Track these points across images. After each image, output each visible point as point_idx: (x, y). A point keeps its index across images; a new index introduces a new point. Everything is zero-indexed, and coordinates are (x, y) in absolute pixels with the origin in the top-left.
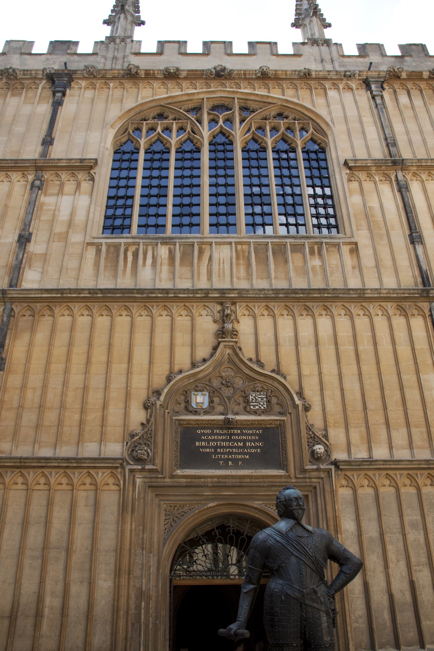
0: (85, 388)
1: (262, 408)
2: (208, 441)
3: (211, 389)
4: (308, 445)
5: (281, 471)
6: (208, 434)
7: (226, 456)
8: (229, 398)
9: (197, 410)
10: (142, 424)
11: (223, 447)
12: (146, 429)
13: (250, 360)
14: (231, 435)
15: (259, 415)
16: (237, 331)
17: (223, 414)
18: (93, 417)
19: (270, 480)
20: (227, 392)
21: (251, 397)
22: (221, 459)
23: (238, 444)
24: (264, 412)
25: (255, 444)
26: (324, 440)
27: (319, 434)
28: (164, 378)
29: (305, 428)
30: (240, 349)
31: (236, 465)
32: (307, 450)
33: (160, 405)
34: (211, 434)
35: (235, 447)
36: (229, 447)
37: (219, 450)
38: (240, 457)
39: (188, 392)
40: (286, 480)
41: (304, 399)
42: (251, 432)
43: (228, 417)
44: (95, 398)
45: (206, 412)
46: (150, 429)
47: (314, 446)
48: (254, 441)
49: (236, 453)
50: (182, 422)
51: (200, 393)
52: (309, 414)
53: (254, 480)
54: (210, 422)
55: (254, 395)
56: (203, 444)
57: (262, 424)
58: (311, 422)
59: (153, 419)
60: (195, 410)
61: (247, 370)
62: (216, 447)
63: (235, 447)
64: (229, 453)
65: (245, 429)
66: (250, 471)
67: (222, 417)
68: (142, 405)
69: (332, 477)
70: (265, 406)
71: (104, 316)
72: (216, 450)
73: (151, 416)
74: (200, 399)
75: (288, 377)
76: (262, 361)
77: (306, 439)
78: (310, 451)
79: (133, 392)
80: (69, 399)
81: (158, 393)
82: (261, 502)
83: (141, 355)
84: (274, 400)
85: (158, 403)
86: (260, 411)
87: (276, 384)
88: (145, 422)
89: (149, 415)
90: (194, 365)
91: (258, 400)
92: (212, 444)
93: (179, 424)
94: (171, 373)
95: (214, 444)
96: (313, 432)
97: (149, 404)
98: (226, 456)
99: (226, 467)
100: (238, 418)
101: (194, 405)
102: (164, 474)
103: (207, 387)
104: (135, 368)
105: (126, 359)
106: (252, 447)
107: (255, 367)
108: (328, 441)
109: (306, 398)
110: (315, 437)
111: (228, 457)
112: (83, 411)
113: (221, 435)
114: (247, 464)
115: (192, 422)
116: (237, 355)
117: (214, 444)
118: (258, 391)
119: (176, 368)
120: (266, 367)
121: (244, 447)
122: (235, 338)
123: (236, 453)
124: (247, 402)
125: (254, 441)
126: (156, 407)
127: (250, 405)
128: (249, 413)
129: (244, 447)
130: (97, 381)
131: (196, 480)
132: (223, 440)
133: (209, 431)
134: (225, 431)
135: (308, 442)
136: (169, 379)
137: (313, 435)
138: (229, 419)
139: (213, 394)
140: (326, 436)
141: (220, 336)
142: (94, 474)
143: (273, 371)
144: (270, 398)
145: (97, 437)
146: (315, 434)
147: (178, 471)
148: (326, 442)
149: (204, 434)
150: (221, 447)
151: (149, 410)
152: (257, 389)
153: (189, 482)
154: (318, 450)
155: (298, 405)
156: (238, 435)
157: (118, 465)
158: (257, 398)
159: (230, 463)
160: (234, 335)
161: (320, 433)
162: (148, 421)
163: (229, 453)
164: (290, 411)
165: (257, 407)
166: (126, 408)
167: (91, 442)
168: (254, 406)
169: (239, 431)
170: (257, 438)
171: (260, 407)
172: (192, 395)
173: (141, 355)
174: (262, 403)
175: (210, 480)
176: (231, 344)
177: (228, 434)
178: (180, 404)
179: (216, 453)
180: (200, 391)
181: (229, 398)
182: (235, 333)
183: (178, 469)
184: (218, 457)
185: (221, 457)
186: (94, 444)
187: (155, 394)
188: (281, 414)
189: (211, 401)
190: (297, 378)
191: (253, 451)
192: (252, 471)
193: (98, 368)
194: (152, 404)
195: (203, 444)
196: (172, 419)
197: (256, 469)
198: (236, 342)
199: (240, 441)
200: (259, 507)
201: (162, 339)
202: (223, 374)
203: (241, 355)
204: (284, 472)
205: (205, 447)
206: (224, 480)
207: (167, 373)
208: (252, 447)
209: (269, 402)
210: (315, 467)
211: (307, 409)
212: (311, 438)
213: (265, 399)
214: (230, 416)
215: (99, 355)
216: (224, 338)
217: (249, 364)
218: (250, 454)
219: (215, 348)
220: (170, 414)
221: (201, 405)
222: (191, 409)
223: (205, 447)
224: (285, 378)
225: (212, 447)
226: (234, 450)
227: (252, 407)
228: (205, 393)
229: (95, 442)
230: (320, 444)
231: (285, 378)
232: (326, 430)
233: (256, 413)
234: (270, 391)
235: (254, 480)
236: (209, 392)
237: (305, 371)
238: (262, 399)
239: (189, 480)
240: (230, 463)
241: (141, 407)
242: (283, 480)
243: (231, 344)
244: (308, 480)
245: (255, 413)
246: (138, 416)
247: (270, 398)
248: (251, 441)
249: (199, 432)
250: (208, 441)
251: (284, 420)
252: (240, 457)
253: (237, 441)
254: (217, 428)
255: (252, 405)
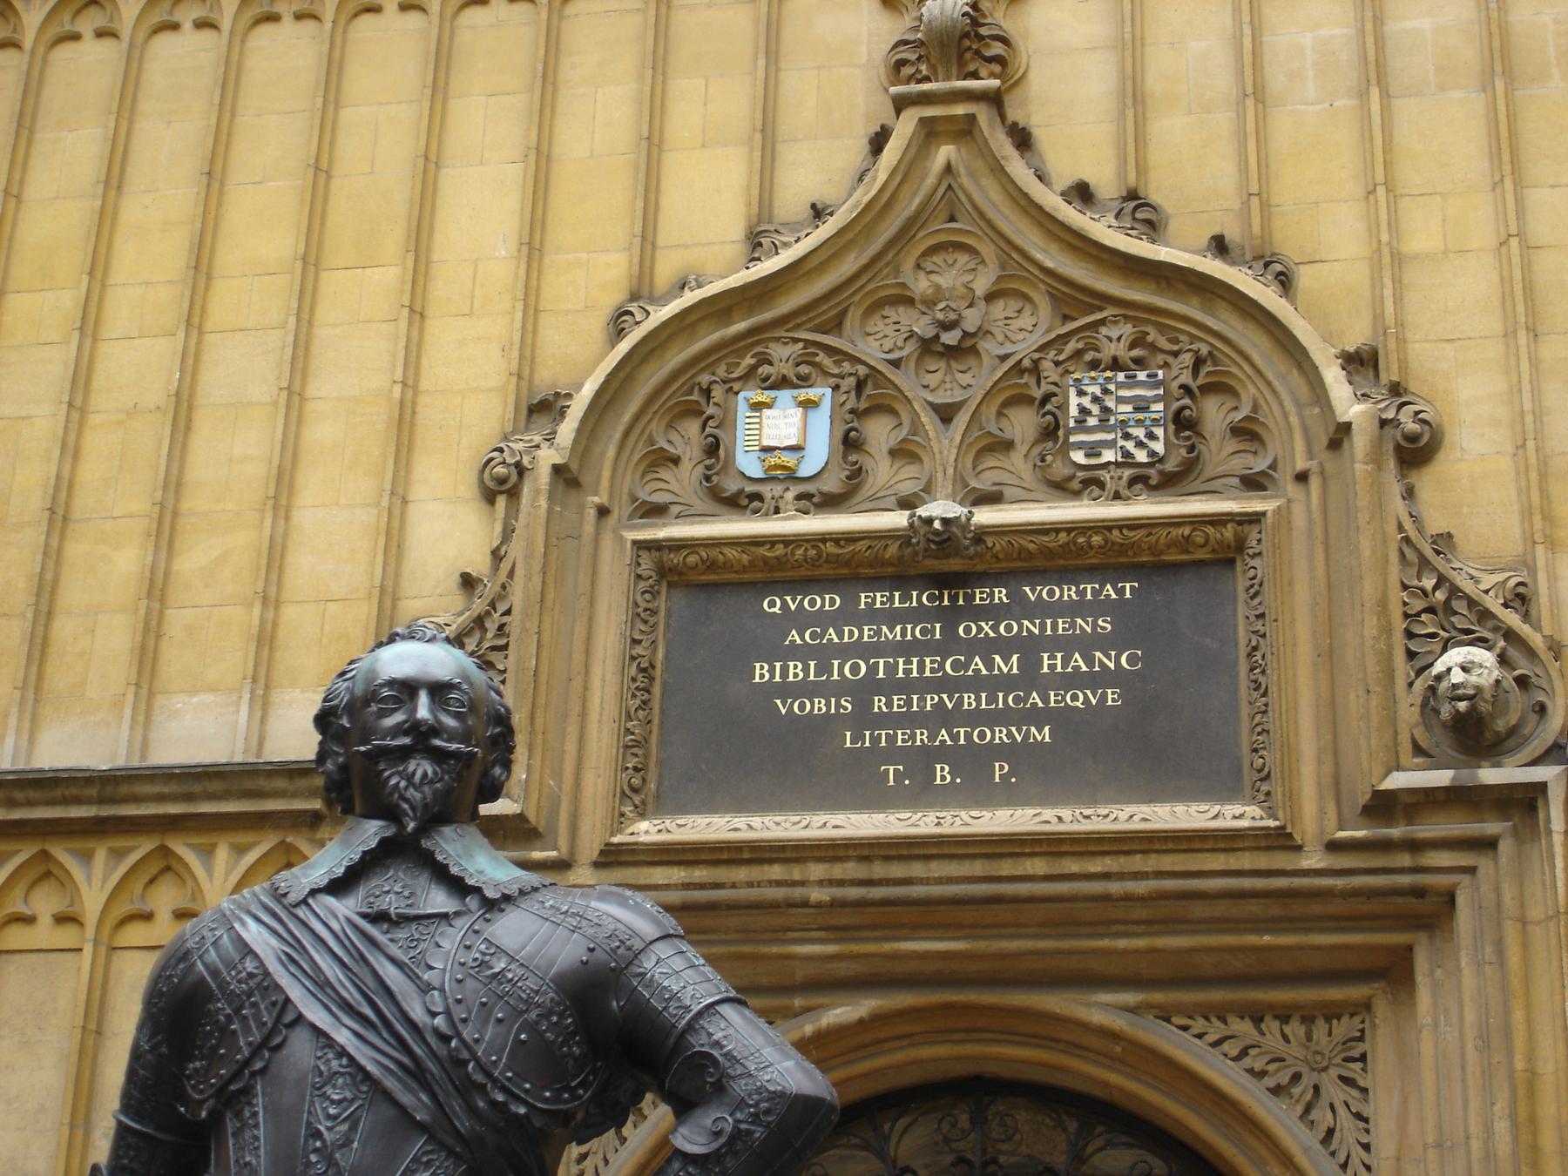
0: (182, 410)
1: (1141, 456)
2: (823, 655)
3: (847, 367)
4: (1411, 655)
5: (1238, 809)
6: (823, 620)
7: (921, 736)
8: (945, 414)
9: (766, 490)
10: (468, 582)
11: (906, 686)
12: (479, 606)
13: (1082, 193)
14: (951, 617)
15: (1117, 496)
16: (1004, 41)
17: (906, 503)
18: (214, 557)
19: (1168, 862)
20: (944, 383)
21: (1074, 401)
22: (892, 753)
23: (989, 664)
24: (1169, 482)
25: (1089, 661)
26: (1512, 619)
27: (1485, 585)
28: (596, 325)
29: (1394, 557)
30: (1023, 139)
31: (975, 776)
32: (1401, 683)
33: (557, 470)
34: (837, 620)
35: (976, 684)
36: (942, 684)
37: (879, 703)
38: (1001, 735)
39: (718, 393)
40: (1262, 861)
41: (1396, 390)
42: (1069, 593)
43: (923, 511)
44: (230, 455)
45: (830, 502)
46: (502, 608)
47: (1444, 650)
48: (1087, 645)
49: (976, 718)
50: (676, 559)
51: (785, 396)
52: (1426, 480)
53: (1074, 866)
54: (830, 548)
55: (1097, 390)
56: (795, 670)
57: (1135, 546)
58: (1436, 523)
59: (515, 550)
60: (750, 488)
61: (1054, 247)
62: (864, 690)
63: (976, 684)
64: (942, 717)
65: (1036, 574)
66: (1048, 813)
67: (898, 519)
68: (472, 479)
69: (1549, 832)
70: (1158, 447)
71: (288, 23)
72: (863, 705)
73: (508, 533)
74: (784, 426)
75: (1305, 278)
76: (1155, 197)
77: (1396, 612)
78: (1420, 685)
79: (429, 411)
80: (92, 471)
81: (545, 408)
82: (1130, 998)
83: (480, 212)
84: (1215, 415)
85: (548, 457)
86: (1127, 473)
87: (1226, 322)
88: (479, 564)
89: (498, 528)
90: (756, 243)
91: (1117, 413)
92: (841, 670)
93: (662, 571)
94: (634, 297)
95: (855, 669)
96: (1441, 580)
97: (500, 470)
98: (921, 736)
99: (922, 793)
100: (985, 516)
101: (749, 464)
102: (563, 843)
103: (822, 358)
104: (446, 286)
105: (394, 239)
106: (1072, 681)
107: (1105, 231)
108: (1537, 627)
109: (1413, 386)
110: (1460, 605)
111: (932, 737)
112: (166, 528)
113: (893, 618)
114: (1038, 773)
115: (731, 553)
116: (998, 170)
117: (855, 669)
118: (1116, 365)
119: (665, 270)
120: (1173, 227)
121: (1030, 678)
122: (993, 75)
123: (976, 718)
124: (1051, 432)
125: (1087, 645)
126: (536, 479)
127: (1067, 446)
128: (1062, 488)
129: (1030, 678)
130: (241, 368)
131: (741, 874)
132: (907, 649)
133: (828, 602)
134: (920, 598)
135: (1410, 635)
136: (618, 324)
137: (1440, 596)
138: (929, 521)
139: (868, 396)
140: (1521, 599)
141: (907, 71)
142: (190, 857)
143: (1220, 246)
144: (1187, 401)
145: (234, 660)
146: (1454, 591)
147: (644, 825)
148: (1525, 630)
149: (801, 620)
150: (893, 686)
151: (501, 501)
152: (1110, 350)
153: (702, 886)
154: (1457, 676)
155: (1346, 428)
156: (993, 613)
157: (317, 805)
158: (1110, 403)
159: (942, 773)
160: (990, 60)
161: (1488, 581)
162: (497, 556)
163: (942, 717)
164: (1301, 465)
165: (1109, 456)
166: (398, 500)
167: (194, 691)
168: (1093, 450)
169: (1001, 594)
170: (1105, 624)
171: (1127, 454)
172: (743, 411)
173: (480, 212)
174: (1139, 433)
175: (816, 871)
176: (960, 110)
177: (938, 614)
178: (676, 461)
179: (863, 718)
180: (783, 383)
181: (945, 414)
182: (997, 49)
183: (642, 814)
184: (875, 740)
185: (891, 739)
186: (208, 698)
187: (542, 421)
188: (1253, 484)
189: (850, 443)
190: (1359, 274)
191: (1079, 700)
192: (1066, 813)
193: (249, 298)
194: (518, 465)
195: (795, 670)
196: (621, 539)
197: (1094, 802)
198: (995, 99)
199: (1004, 646)
200: (1118, 1022)
201: (598, 116)
202: (921, 285)
203: (1018, 169)
204: (1254, 810)
205: (805, 690)
206: (897, 870)
207: (611, 299)
208: (1072, 681)
209: (1183, 423)
210: (1442, 778)
211: (1415, 451)
212: (1430, 610)
213: (1159, 407)
214: (940, 508)
215: (260, 233)
216: (927, 79)
217: (1071, 214)
218: (1060, 719)
219: (878, 142)
220: (612, 520)
221: (788, 459)
222: (731, 486)
223: (805, 690)
224: (1285, 282)
225: (843, 688)
226: (969, 701)
227: (1078, 457)
228: (811, 393)
229: (212, 689)
230: (1482, 642)
231: (1285, 282)
232: (1527, 564)
233: (1101, 485)
234: (1187, 359)
235: (1074, 866)
236: (836, 388)
237: (1422, 236)
238: (1141, 406)
239: (700, 874)
240: (942, 773)
241: (468, 488)
242: (1246, 861)
243: (960, 110)
244: (1405, 860)
245: (1090, 483)
246: (450, 534)
247: (1187, 401)
248: (1066, 645)
249: (772, 606)
250: (823, 655)
251: (1256, 518)
252: (1001, 735)
253: (987, 648)
254: (874, 582)
255: (1080, 446)
